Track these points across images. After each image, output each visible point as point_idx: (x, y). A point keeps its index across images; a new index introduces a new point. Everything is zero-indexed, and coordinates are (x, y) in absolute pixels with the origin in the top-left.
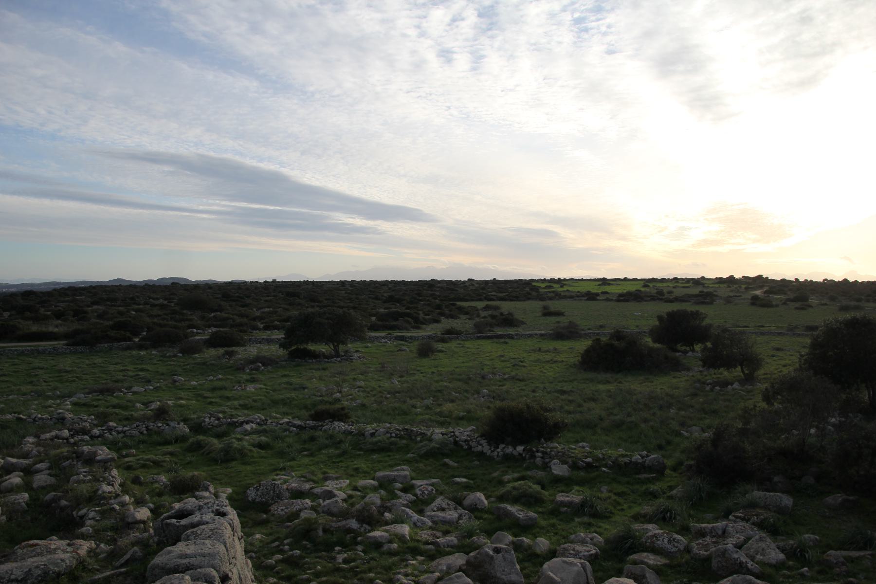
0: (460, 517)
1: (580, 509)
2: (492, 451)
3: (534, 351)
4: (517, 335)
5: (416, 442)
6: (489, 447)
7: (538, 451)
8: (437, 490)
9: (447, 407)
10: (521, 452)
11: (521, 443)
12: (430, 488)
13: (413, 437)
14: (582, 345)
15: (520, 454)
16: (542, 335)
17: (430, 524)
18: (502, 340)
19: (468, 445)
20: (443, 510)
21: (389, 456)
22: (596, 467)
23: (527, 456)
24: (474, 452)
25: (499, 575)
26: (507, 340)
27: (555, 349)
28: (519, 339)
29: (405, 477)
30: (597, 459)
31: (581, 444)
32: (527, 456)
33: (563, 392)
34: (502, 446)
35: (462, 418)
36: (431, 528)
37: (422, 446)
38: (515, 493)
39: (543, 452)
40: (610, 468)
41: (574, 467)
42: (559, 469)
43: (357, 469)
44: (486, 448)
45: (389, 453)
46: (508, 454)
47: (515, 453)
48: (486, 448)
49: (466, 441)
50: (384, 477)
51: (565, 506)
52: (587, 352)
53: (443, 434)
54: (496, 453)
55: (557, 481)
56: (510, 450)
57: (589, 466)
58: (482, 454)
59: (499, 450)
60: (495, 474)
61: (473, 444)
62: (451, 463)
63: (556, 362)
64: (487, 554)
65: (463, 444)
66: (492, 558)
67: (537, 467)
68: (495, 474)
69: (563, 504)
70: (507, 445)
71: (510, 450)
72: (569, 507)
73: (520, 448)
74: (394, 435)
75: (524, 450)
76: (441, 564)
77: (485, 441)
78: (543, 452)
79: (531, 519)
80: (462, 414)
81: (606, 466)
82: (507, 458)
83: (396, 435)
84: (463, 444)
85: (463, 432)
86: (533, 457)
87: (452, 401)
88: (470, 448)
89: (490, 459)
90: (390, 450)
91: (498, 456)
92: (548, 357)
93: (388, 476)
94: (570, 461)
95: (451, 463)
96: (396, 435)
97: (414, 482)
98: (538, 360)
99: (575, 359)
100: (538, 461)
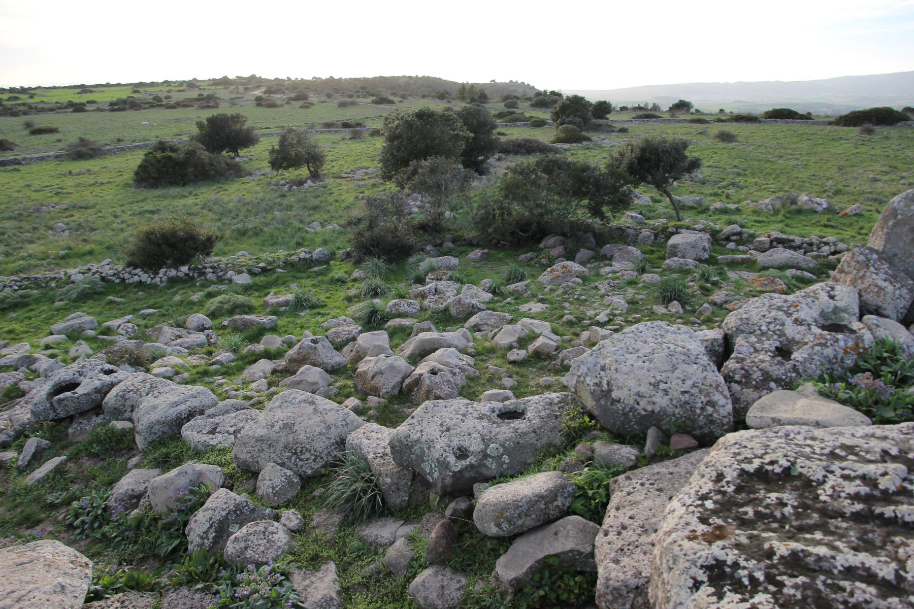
0: (208, 336)
1: (299, 304)
2: (152, 279)
3: (65, 175)
4: (24, 159)
5: (52, 289)
6: (147, 275)
7: (205, 268)
8: (138, 326)
9: (32, 248)
10: (187, 272)
11: (183, 263)
12: (130, 325)
13: (44, 285)
14: (136, 159)
15: (186, 274)
16: (57, 157)
17: (186, 351)
18: (10, 168)
19: (119, 278)
20: (180, 337)
21: (33, 310)
22: (270, 270)
23: (196, 275)
24: (130, 284)
25: (325, 361)
26: (17, 167)
27: (89, 170)
28: (30, 164)
29: (92, 322)
30: (269, 263)
31: (240, 253)
32: (196, 275)
33: (152, 212)
34: (162, 271)
35: (63, 258)
36: (190, 354)
37: (68, 291)
38: (226, 306)
39: (211, 267)
40: (283, 268)
41: (251, 273)
42: (243, 279)
43: (10, 332)
44: (145, 277)
45: (30, 307)
46: (172, 277)
47: (180, 274)
48: (145, 277)
49: (115, 274)
50: (66, 329)
51: (282, 306)
52: (142, 167)
53: (83, 273)
54: (158, 279)
55: (247, 289)
56: (173, 273)
57: (264, 270)
58: (141, 284)
59: (160, 275)
60: (177, 298)
61: (126, 276)
62: (118, 300)
63: (102, 184)
64: (311, 347)
65: (113, 278)
66: (315, 348)
67: (213, 283)
68: (177, 298)
69: (280, 305)
70: (169, 267)
71: (173, 273)
72: (286, 306)
73: (185, 269)
74: (16, 288)
75: (189, 269)
76: (254, 373)
77: (139, 270)
78: (211, 267)
79: (273, 321)
80: (62, 252)
81: (279, 267)
82: (173, 281)
83: (20, 287)
84: (113, 278)
85: (107, 267)
86: (202, 273)
87: (31, 242)
88: (123, 280)
89: (154, 287)
90: (27, 305)
91: (161, 282)
92: (91, 180)
93: (72, 326)
94: (244, 269)
95: (118, 300)
96: (20, 287)
97: (108, 323)
98: (79, 185)
99: (129, 176)
100: (211, 276)
